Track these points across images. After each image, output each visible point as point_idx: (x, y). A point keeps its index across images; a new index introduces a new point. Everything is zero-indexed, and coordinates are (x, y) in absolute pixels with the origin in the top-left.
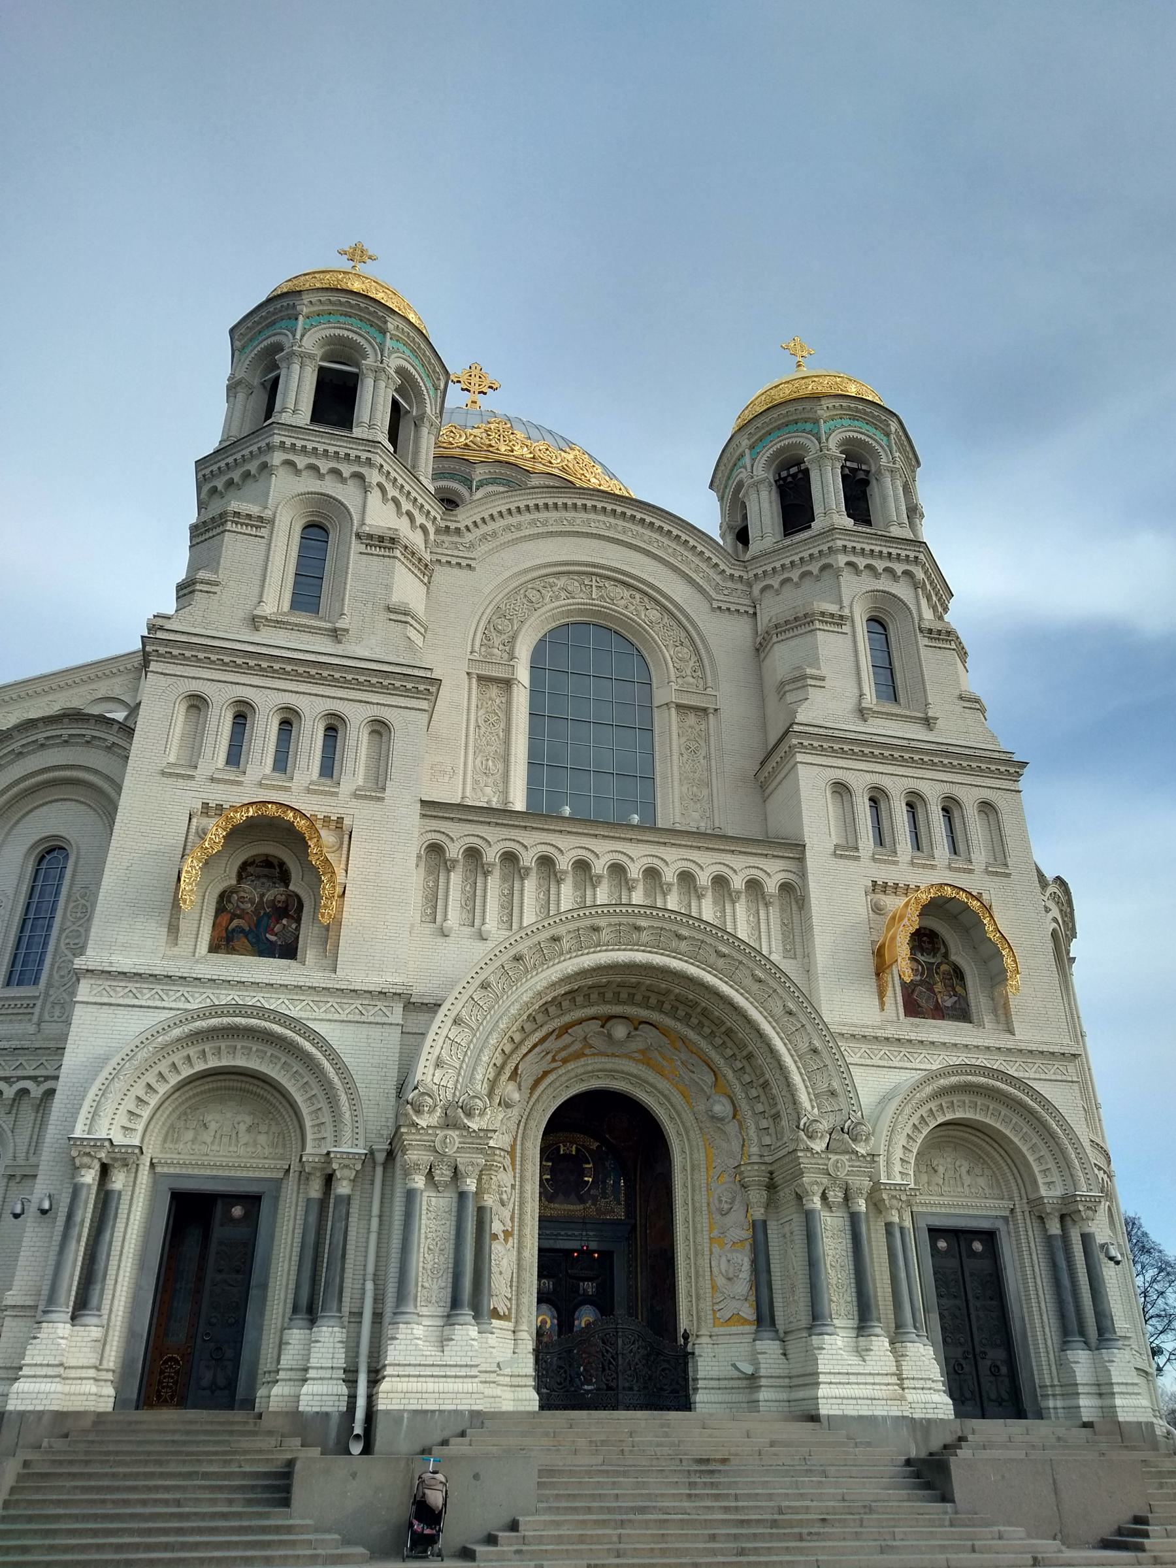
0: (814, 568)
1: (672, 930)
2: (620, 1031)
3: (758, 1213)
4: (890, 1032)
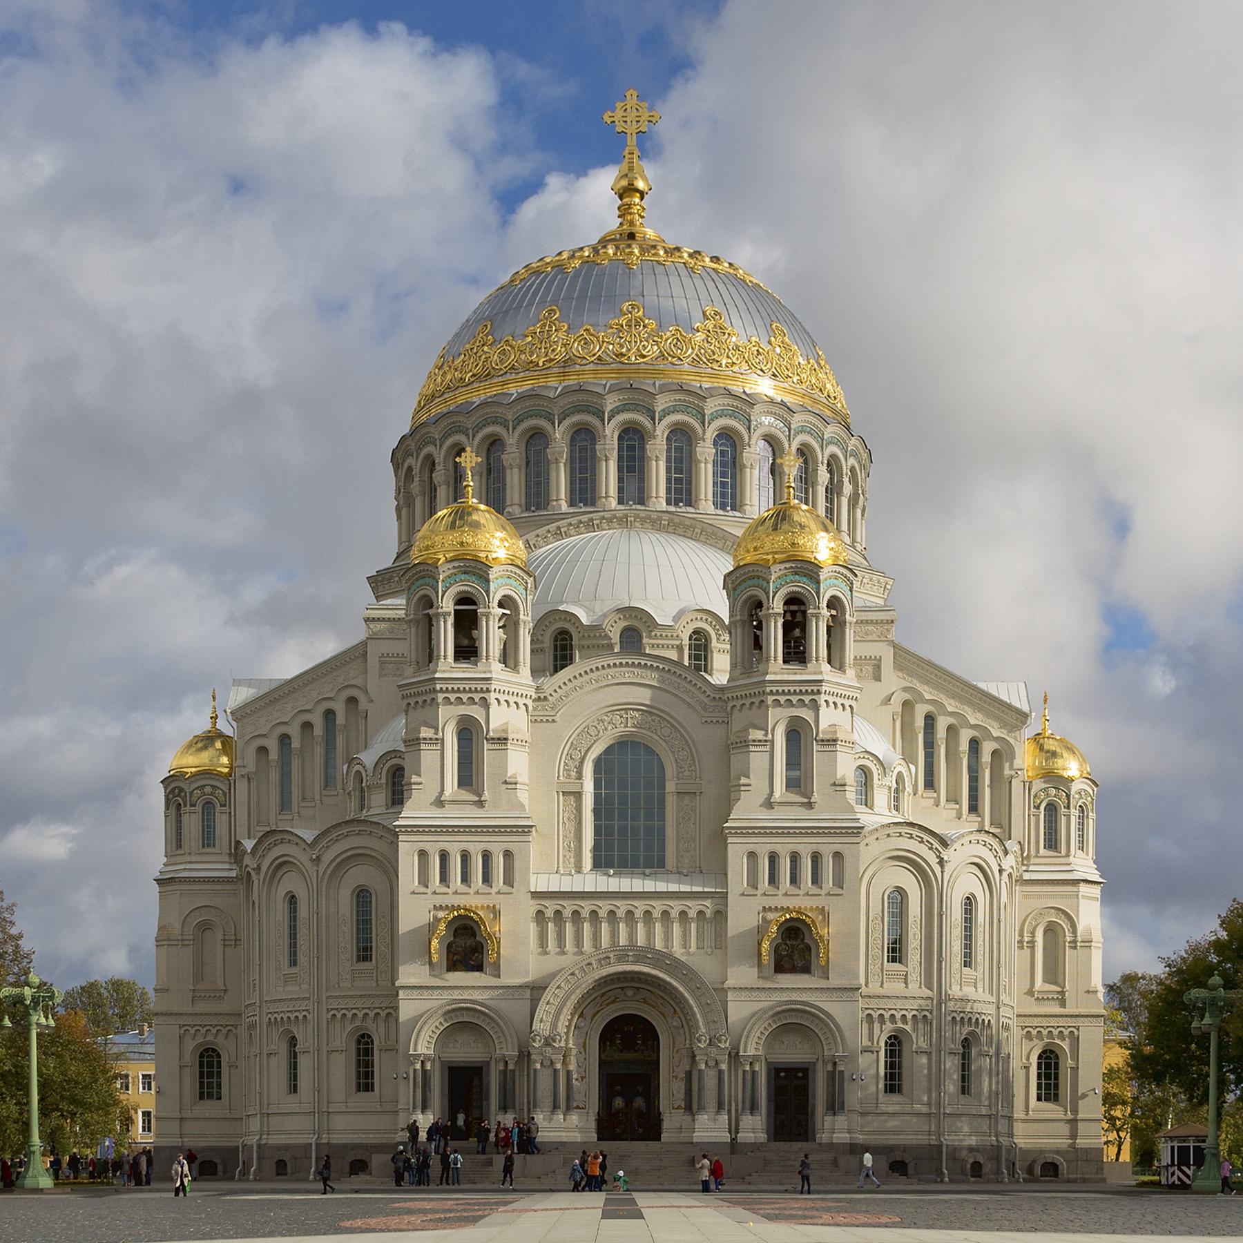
0: (756, 700)
1: (642, 955)
2: (630, 993)
3: (688, 1068)
4: (761, 984)
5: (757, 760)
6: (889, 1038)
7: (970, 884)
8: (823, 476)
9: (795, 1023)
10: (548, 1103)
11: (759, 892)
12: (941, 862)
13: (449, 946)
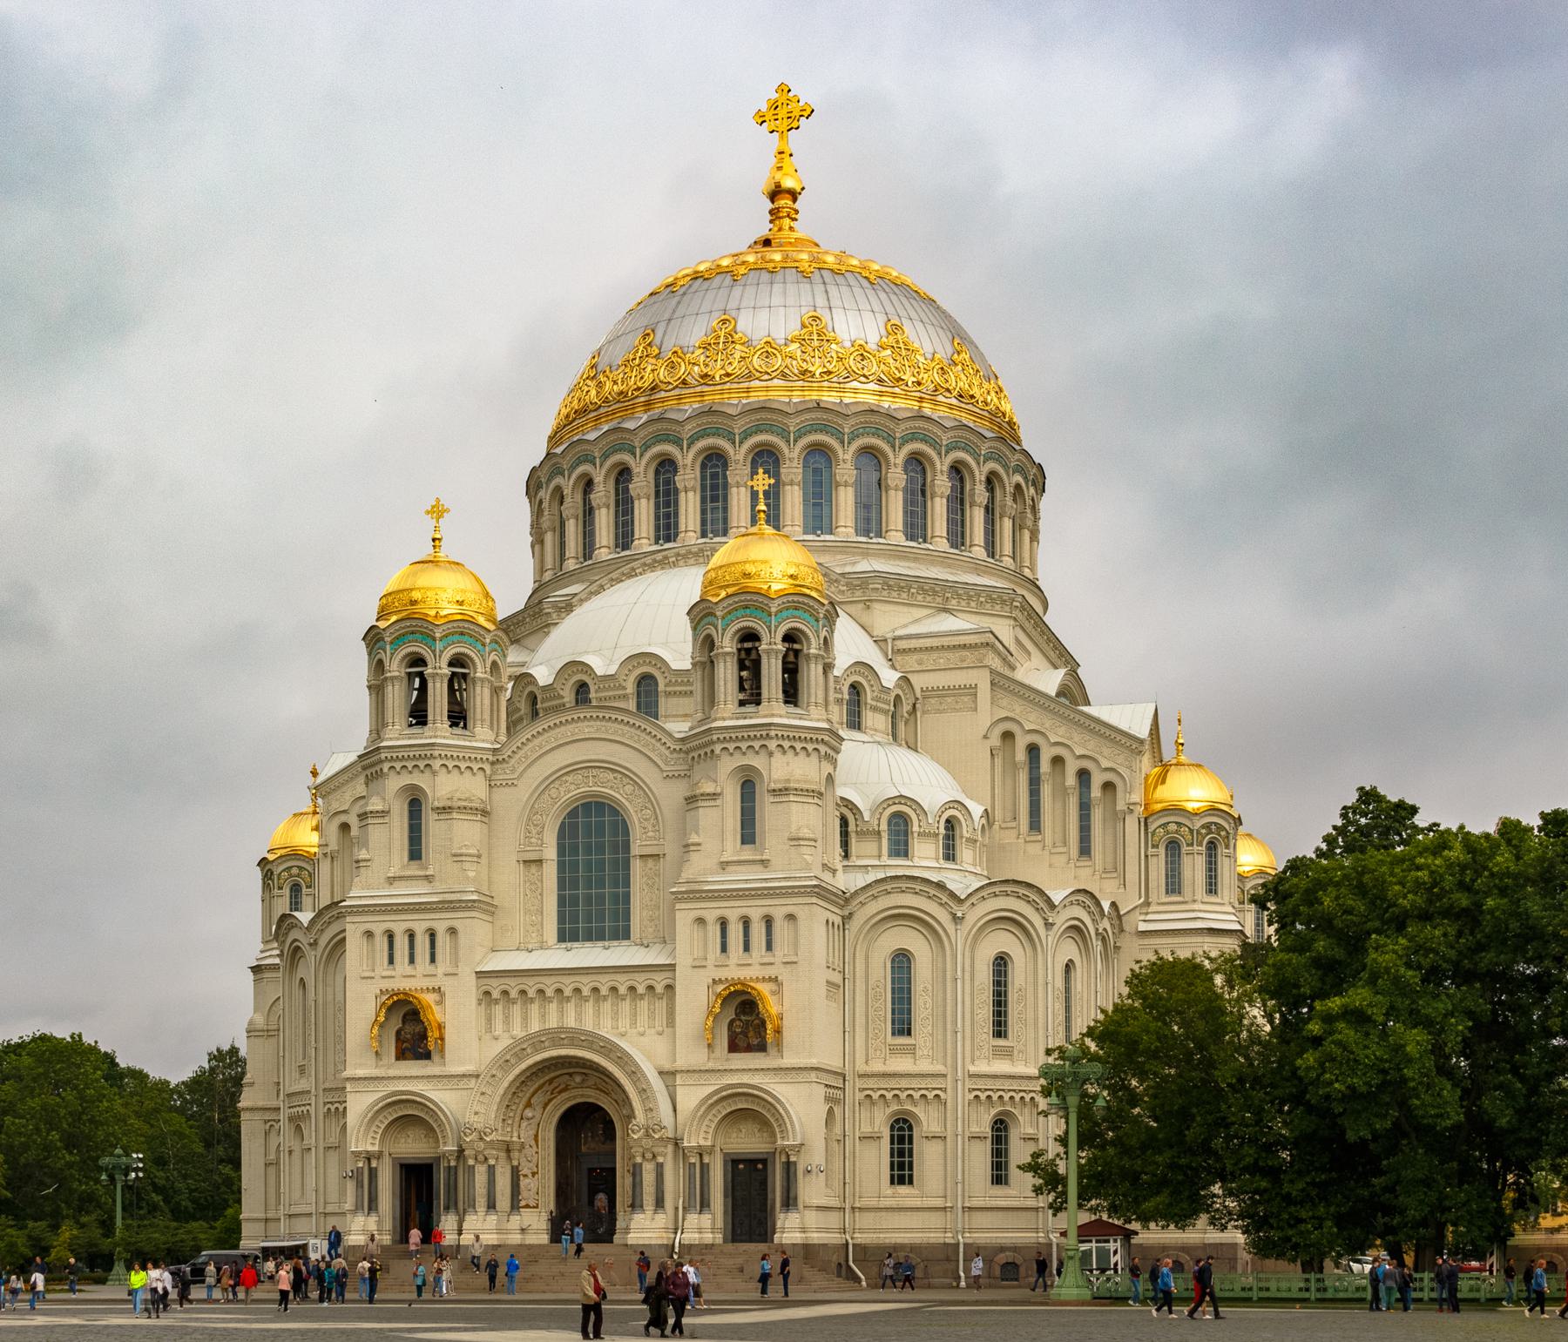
2: (578, 1079)
4: (710, 1065)
5: (706, 816)
6: (897, 1121)
7: (1003, 941)
8: (942, 484)
9: (748, 1110)
10: (481, 1202)
11: (710, 962)
12: (956, 919)
13: (398, 1033)
